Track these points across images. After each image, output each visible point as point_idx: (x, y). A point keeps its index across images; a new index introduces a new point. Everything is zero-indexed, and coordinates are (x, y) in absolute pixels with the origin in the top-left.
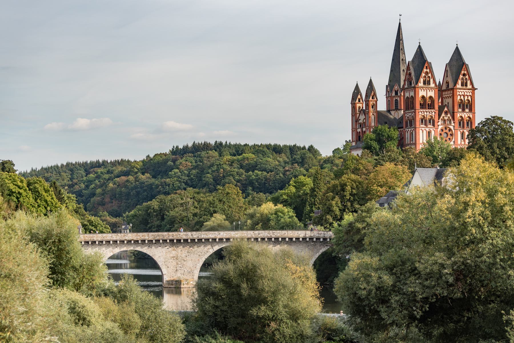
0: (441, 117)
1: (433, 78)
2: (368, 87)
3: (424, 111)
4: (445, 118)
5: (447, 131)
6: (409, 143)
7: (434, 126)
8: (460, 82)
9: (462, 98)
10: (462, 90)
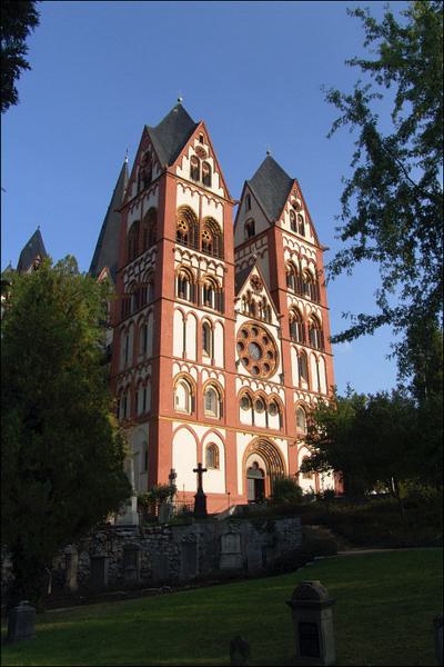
0: (243, 292)
1: (220, 174)
2: (28, 245)
3: (192, 252)
4: (254, 296)
5: (259, 339)
6: (130, 364)
7: (223, 312)
8: (287, 216)
9: (295, 258)
10: (295, 240)
